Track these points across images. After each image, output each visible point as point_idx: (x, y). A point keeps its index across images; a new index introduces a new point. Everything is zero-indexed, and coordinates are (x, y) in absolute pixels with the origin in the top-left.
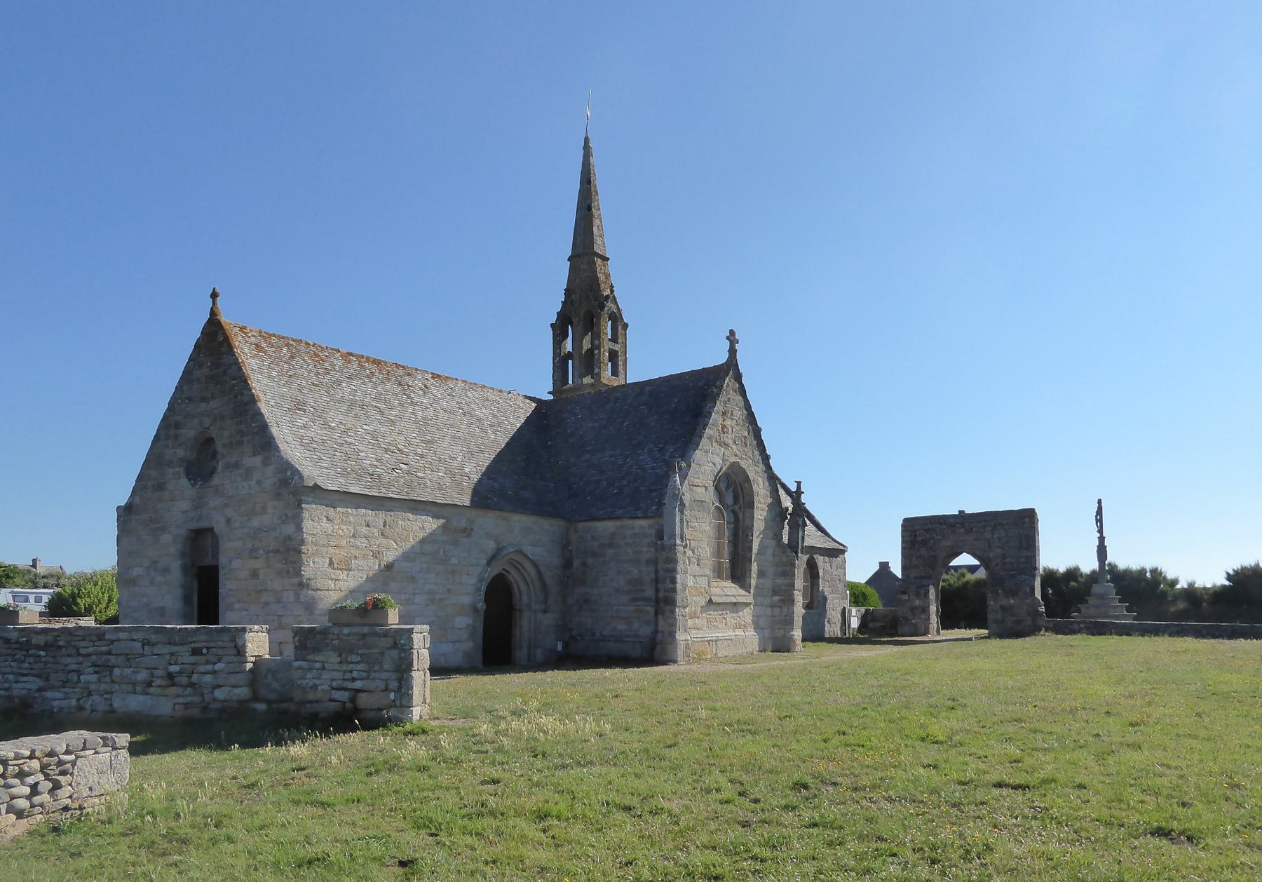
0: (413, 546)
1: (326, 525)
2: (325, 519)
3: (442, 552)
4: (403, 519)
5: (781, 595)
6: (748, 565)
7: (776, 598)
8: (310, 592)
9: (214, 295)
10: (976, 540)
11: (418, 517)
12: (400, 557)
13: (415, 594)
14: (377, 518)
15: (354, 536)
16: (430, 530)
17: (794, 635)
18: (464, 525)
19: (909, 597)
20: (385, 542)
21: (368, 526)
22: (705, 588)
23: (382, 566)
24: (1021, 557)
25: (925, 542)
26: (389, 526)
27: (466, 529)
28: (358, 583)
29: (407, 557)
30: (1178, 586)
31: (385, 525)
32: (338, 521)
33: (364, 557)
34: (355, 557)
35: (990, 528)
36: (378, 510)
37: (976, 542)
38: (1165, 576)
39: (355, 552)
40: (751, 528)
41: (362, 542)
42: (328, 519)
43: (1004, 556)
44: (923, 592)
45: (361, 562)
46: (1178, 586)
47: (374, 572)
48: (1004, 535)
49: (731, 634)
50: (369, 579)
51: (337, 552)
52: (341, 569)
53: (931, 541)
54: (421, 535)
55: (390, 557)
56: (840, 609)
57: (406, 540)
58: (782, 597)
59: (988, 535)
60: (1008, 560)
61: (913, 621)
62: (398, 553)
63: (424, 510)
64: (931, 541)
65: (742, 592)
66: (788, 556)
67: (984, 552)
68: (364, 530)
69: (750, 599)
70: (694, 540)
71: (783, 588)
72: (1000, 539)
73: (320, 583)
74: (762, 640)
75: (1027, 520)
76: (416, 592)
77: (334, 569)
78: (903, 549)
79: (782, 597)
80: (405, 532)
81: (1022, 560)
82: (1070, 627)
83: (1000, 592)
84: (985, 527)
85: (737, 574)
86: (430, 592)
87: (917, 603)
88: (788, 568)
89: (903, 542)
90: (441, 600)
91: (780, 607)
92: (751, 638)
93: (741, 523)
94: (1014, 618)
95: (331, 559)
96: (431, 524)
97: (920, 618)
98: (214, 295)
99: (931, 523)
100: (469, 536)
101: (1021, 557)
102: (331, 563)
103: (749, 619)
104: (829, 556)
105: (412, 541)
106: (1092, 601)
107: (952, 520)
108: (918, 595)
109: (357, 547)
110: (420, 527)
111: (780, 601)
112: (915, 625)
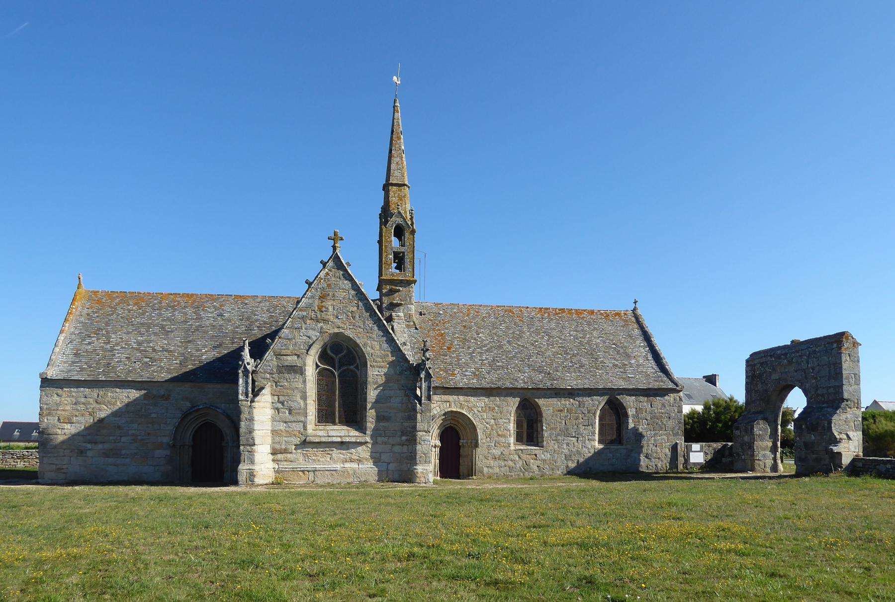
0: (120, 408)
1: (55, 397)
2: (56, 396)
3: (143, 410)
4: (112, 392)
5: (408, 436)
6: (364, 412)
7: (404, 438)
8: (45, 436)
9: (335, 238)
10: (796, 371)
11: (124, 390)
12: (110, 414)
13: (121, 437)
14: (95, 393)
15: (75, 404)
16: (134, 398)
17: (416, 469)
18: (163, 393)
19: (741, 432)
20: (98, 406)
21: (86, 397)
22: (299, 431)
23: (96, 420)
25: (760, 376)
26: (101, 397)
27: (164, 395)
28: (78, 430)
29: (115, 414)
31: (98, 397)
32: (64, 395)
33: (83, 415)
34: (76, 415)
36: (93, 388)
37: (795, 374)
39: (75, 413)
40: (365, 383)
41: (82, 407)
42: (58, 395)
44: (749, 427)
45: (80, 419)
47: (90, 424)
48: (816, 364)
49: (338, 466)
50: (86, 429)
51: (63, 413)
52: (66, 423)
53: (765, 375)
54: (126, 401)
55: (103, 415)
57: (114, 404)
58: (409, 437)
61: (743, 457)
62: (109, 412)
63: (129, 386)
64: (765, 375)
65: (357, 433)
66: (412, 403)
68: (83, 400)
69: (368, 439)
70: (281, 395)
71: (409, 429)
73: (51, 431)
74: (380, 473)
75: (835, 345)
76: (121, 435)
77: (60, 423)
78: (747, 384)
79: (409, 437)
80: (114, 400)
81: (831, 390)
83: (804, 426)
85: (354, 419)
86: (133, 435)
87: (746, 438)
88: (412, 413)
89: (747, 377)
90: (142, 440)
91: (408, 445)
92: (368, 469)
93: (359, 379)
95: (59, 417)
96: (134, 394)
98: (335, 238)
99: (765, 356)
100: (167, 399)
102: (59, 419)
103: (367, 455)
104: (648, 396)
105: (119, 405)
107: (779, 352)
108: (746, 431)
109: (78, 410)
110: (125, 396)
111: (407, 440)
112: (744, 460)
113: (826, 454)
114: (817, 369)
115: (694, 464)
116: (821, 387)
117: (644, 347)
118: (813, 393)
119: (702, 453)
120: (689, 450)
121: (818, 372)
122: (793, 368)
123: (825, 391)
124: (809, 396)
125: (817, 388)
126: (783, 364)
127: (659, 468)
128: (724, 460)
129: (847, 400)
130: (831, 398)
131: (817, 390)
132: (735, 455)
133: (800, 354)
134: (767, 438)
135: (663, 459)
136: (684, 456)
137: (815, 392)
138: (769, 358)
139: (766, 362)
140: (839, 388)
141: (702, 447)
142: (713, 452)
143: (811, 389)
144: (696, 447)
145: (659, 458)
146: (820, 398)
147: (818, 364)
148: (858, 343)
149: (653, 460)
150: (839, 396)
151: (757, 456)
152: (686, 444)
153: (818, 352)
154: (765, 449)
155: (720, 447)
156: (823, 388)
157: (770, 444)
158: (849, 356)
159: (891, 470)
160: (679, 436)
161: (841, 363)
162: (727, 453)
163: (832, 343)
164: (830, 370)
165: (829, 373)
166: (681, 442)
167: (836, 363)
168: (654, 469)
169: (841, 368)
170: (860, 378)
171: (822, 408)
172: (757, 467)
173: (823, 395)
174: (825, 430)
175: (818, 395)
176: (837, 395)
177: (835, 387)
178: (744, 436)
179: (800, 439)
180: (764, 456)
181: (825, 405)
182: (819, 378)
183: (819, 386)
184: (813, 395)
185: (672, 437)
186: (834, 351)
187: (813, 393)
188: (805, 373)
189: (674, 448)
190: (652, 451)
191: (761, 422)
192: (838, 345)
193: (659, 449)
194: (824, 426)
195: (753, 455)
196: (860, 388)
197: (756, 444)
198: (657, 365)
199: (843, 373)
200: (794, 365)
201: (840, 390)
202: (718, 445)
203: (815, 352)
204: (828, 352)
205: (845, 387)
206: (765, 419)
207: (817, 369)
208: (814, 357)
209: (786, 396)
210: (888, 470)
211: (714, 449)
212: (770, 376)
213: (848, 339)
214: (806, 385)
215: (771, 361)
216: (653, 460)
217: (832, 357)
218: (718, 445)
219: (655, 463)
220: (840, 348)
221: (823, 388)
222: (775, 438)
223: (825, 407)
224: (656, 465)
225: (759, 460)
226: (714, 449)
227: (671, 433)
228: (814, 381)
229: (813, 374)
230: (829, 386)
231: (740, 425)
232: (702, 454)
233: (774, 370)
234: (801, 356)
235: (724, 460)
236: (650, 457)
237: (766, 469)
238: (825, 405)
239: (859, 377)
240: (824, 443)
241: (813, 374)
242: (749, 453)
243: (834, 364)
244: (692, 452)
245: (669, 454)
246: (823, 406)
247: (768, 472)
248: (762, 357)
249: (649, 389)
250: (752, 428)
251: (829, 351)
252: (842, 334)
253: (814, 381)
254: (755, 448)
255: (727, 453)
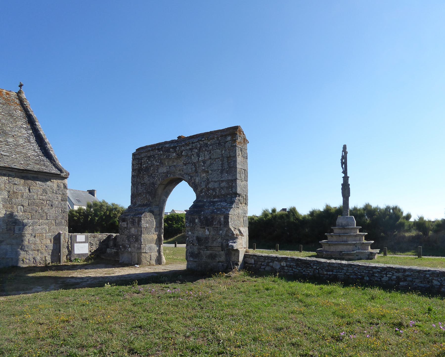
10: (185, 164)
19: (127, 224)
24: (222, 181)
30: (412, 220)
35: (196, 151)
38: (399, 208)
43: (208, 182)
44: (137, 220)
46: (412, 220)
56: (51, 235)
59: (195, 159)
60: (210, 186)
61: (130, 249)
67: (191, 177)
72: (204, 162)
75: (229, 138)
81: (223, 184)
82: (271, 264)
84: (191, 149)
87: (133, 231)
94: (209, 252)
97: (134, 247)
101: (222, 181)
106: (336, 230)
108: (133, 223)
113: (222, 251)
114: (208, 163)
115: (79, 255)
116: (212, 181)
117: (26, 129)
118: (204, 187)
119: (87, 245)
120: (73, 241)
121: (210, 166)
122: (183, 162)
123: (216, 185)
124: (199, 189)
125: (208, 182)
126: (171, 158)
127: (38, 261)
128: (108, 250)
129: (239, 195)
130: (223, 192)
131: (208, 183)
132: (121, 247)
133: (190, 147)
134: (153, 230)
135: (44, 251)
136: (68, 247)
137: (206, 186)
138: (157, 151)
139: (153, 155)
140: (233, 183)
141: (87, 238)
142: (98, 243)
143: (201, 183)
144: (81, 237)
145: (38, 250)
146: (211, 192)
147: (210, 157)
148: (247, 140)
149: (31, 252)
150: (232, 191)
151: (144, 249)
152: (70, 234)
153: (210, 145)
154: (151, 242)
155: (105, 238)
156: (215, 182)
157: (155, 237)
158: (241, 151)
159: (286, 268)
160: (63, 225)
161: (235, 157)
162: (111, 243)
163: (226, 136)
164: (222, 164)
165: (222, 167)
166: (65, 232)
167: (230, 157)
168: (32, 262)
169: (235, 161)
170: (247, 174)
171: (214, 202)
172: (144, 261)
173: (214, 190)
174: (221, 225)
175: (208, 189)
176: (230, 190)
177: (228, 181)
178: (130, 228)
179: (193, 233)
180: (150, 248)
181: (216, 200)
182: (210, 172)
183: (210, 180)
184: (203, 189)
185: (55, 227)
186: (227, 144)
187: (204, 187)
188: (195, 165)
189: (57, 239)
190: (29, 242)
191: (148, 214)
192: (232, 137)
193: (38, 240)
194: (220, 222)
195: (140, 248)
196: (247, 184)
197: (143, 237)
198: (40, 149)
199: (237, 166)
200: (183, 158)
201: (234, 184)
202: (103, 236)
203: (206, 145)
204: (221, 145)
205: (238, 181)
206: (152, 212)
207: (208, 163)
208: (206, 150)
209: (171, 191)
210: (282, 267)
211: (99, 240)
212: (157, 170)
213: (240, 134)
214: (195, 179)
215: (158, 154)
216: (31, 252)
217: (225, 151)
218: (103, 236)
219: (34, 256)
220: (235, 141)
221: (215, 182)
222: (160, 231)
223: (217, 202)
224: (34, 258)
225: (145, 252)
226: (99, 240)
227: (54, 223)
228: (205, 175)
229: (204, 168)
230: (221, 179)
231: (126, 217)
232: (87, 245)
233: (161, 163)
234: (191, 149)
235: (108, 250)
236: (27, 249)
237: (151, 262)
238: (216, 200)
239: (247, 172)
240: (220, 239)
241: (204, 168)
242: (136, 245)
243: (229, 158)
244: (77, 243)
245: (51, 246)
246: (214, 200)
247: (153, 265)
248: (149, 151)
249: (26, 170)
250: (140, 220)
251: (222, 144)
252: (236, 129)
253: (205, 175)
254: (142, 241)
255: (111, 243)
